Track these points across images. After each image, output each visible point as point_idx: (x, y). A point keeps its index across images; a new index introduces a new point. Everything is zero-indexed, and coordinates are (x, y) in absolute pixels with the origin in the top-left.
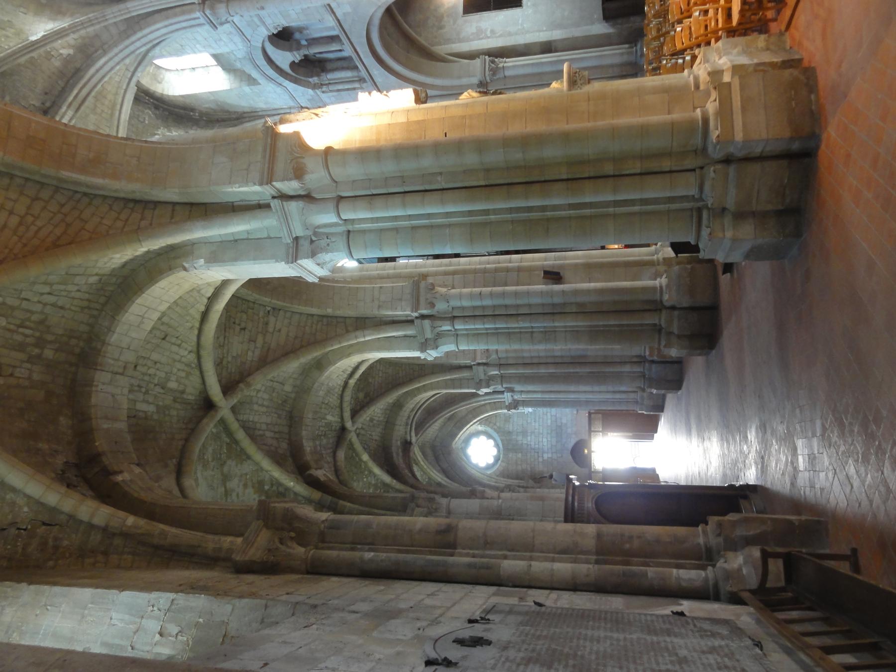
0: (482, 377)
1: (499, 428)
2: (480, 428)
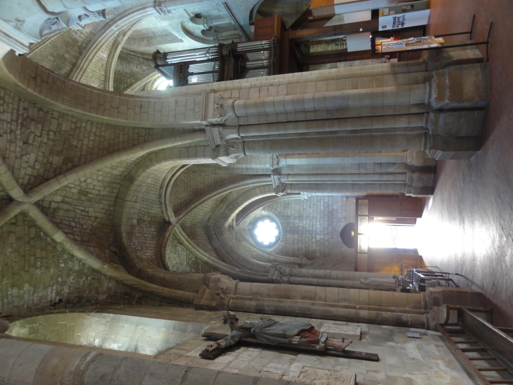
0: (219, 142)
1: (280, 213)
2: (264, 213)
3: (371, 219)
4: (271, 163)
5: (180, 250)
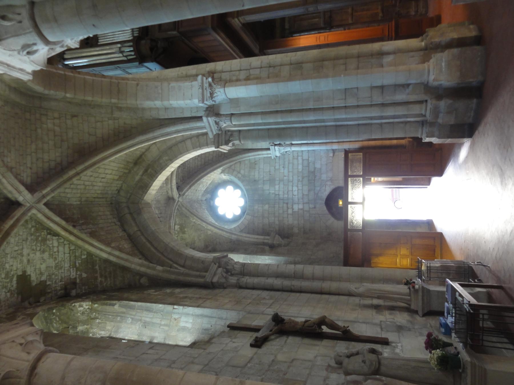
1: (244, 176)
2: (225, 177)
3: (366, 182)
4: (201, 96)
5: (56, 244)
